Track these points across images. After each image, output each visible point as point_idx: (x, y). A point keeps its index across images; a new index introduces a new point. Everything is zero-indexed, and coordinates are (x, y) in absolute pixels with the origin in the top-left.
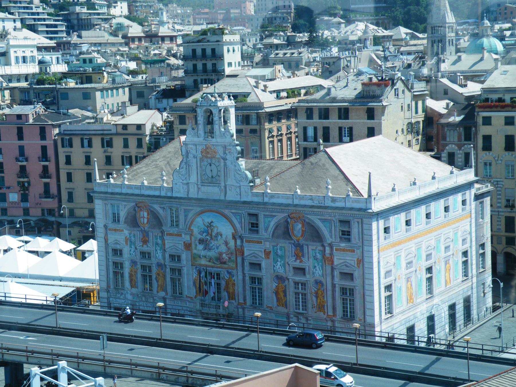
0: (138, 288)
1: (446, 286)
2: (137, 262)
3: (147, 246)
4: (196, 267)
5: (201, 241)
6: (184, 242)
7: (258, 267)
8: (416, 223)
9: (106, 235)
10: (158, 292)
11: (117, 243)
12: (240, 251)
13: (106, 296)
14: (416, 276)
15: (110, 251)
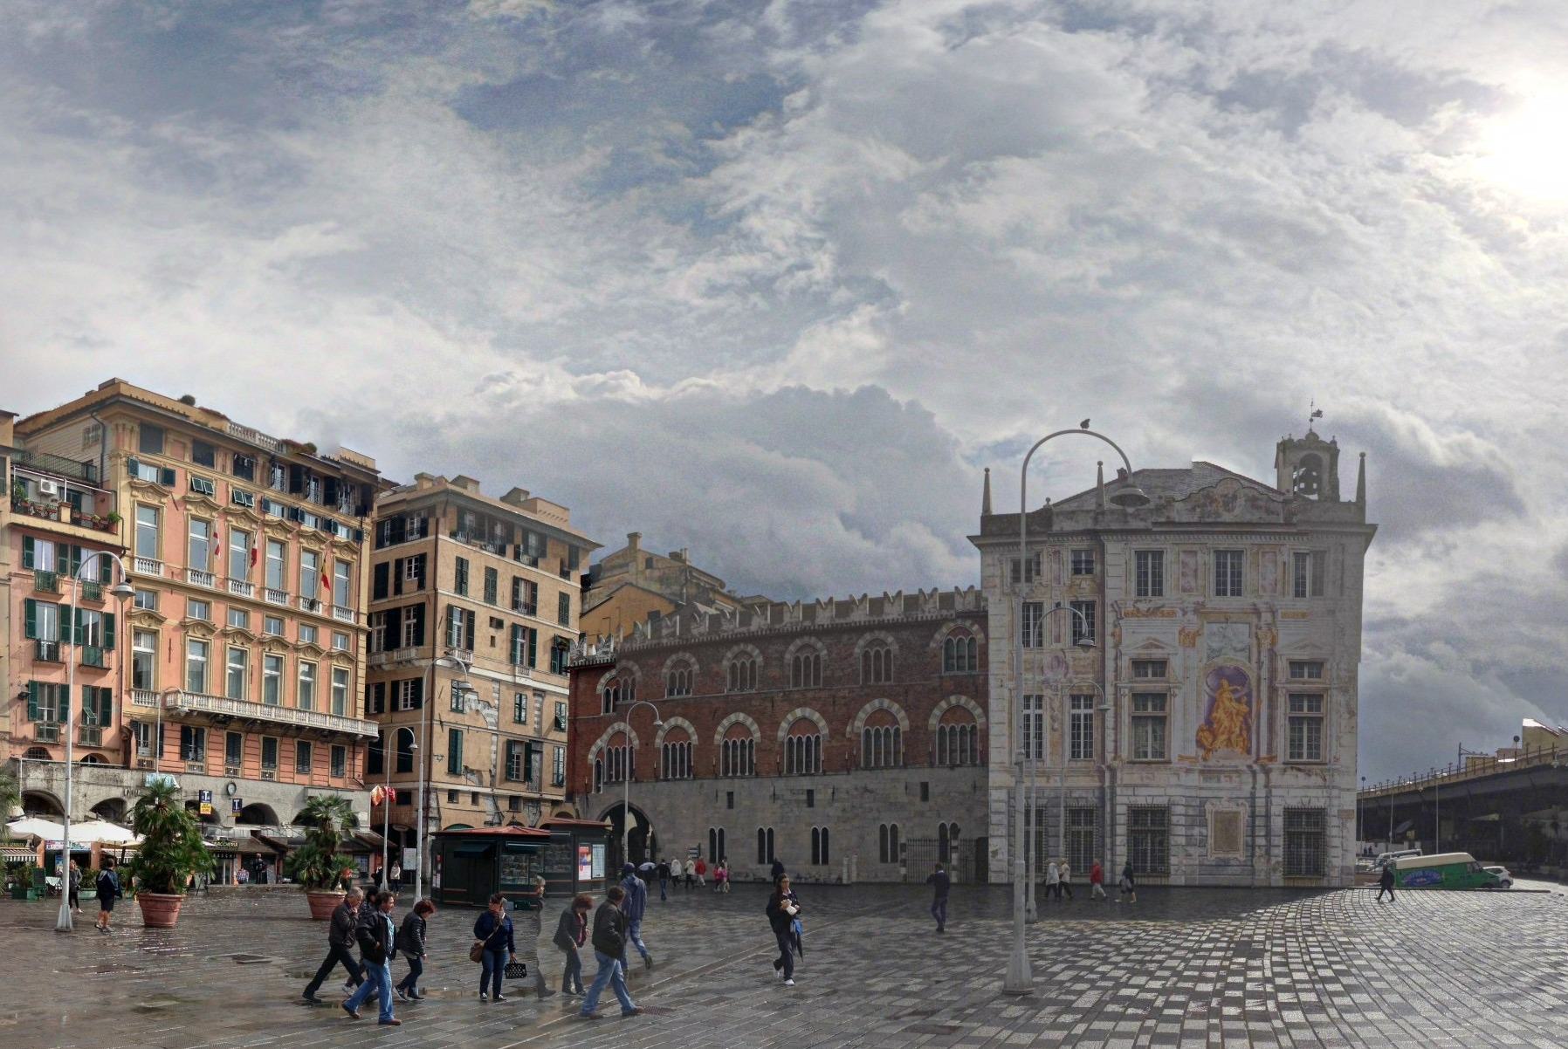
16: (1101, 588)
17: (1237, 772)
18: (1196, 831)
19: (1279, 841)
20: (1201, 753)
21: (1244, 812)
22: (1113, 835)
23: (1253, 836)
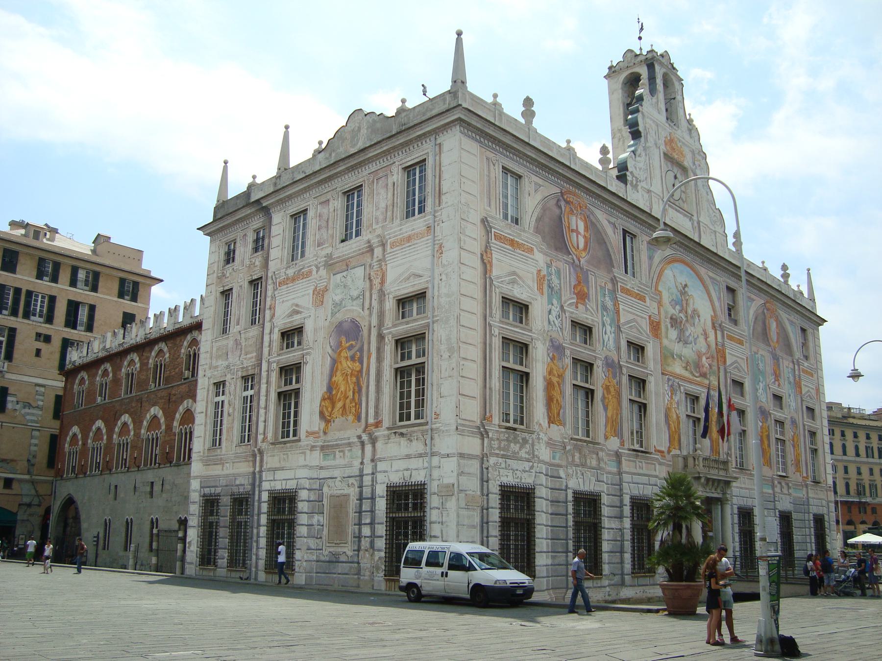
0: (564, 425)
2: (564, 348)
3: (587, 309)
4: (669, 380)
5: (674, 322)
6: (650, 317)
7: (738, 389)
9: (487, 248)
10: (606, 438)
11: (513, 282)
12: (721, 354)
13: (477, 451)
15: (497, 301)
16: (266, 260)
17: (349, 444)
18: (316, 518)
19: (381, 530)
20: (323, 425)
21: (353, 492)
22: (259, 525)
23: (360, 524)
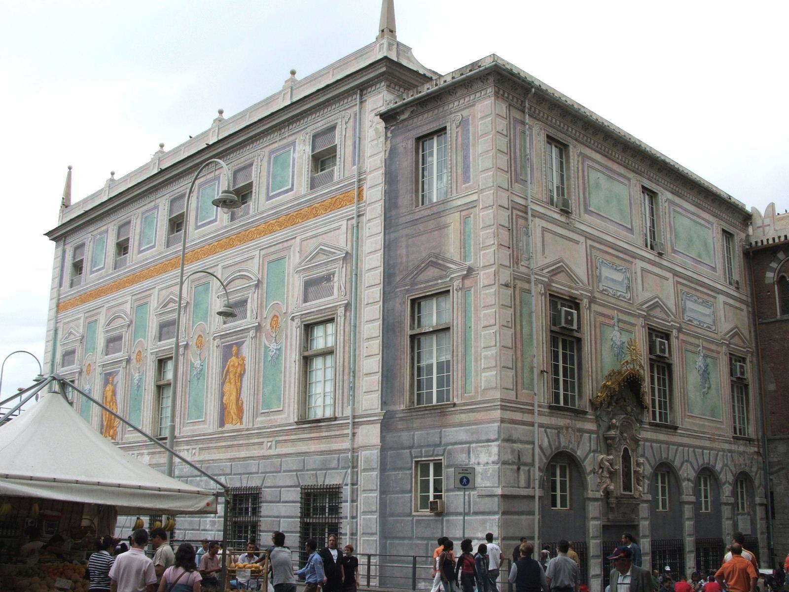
1: (222, 423)
8: (140, 245)
14: (128, 376)
